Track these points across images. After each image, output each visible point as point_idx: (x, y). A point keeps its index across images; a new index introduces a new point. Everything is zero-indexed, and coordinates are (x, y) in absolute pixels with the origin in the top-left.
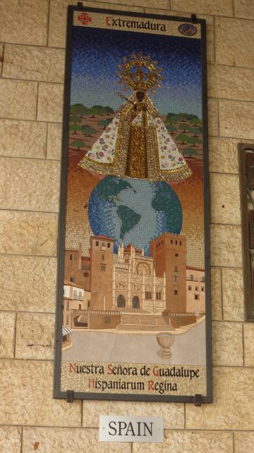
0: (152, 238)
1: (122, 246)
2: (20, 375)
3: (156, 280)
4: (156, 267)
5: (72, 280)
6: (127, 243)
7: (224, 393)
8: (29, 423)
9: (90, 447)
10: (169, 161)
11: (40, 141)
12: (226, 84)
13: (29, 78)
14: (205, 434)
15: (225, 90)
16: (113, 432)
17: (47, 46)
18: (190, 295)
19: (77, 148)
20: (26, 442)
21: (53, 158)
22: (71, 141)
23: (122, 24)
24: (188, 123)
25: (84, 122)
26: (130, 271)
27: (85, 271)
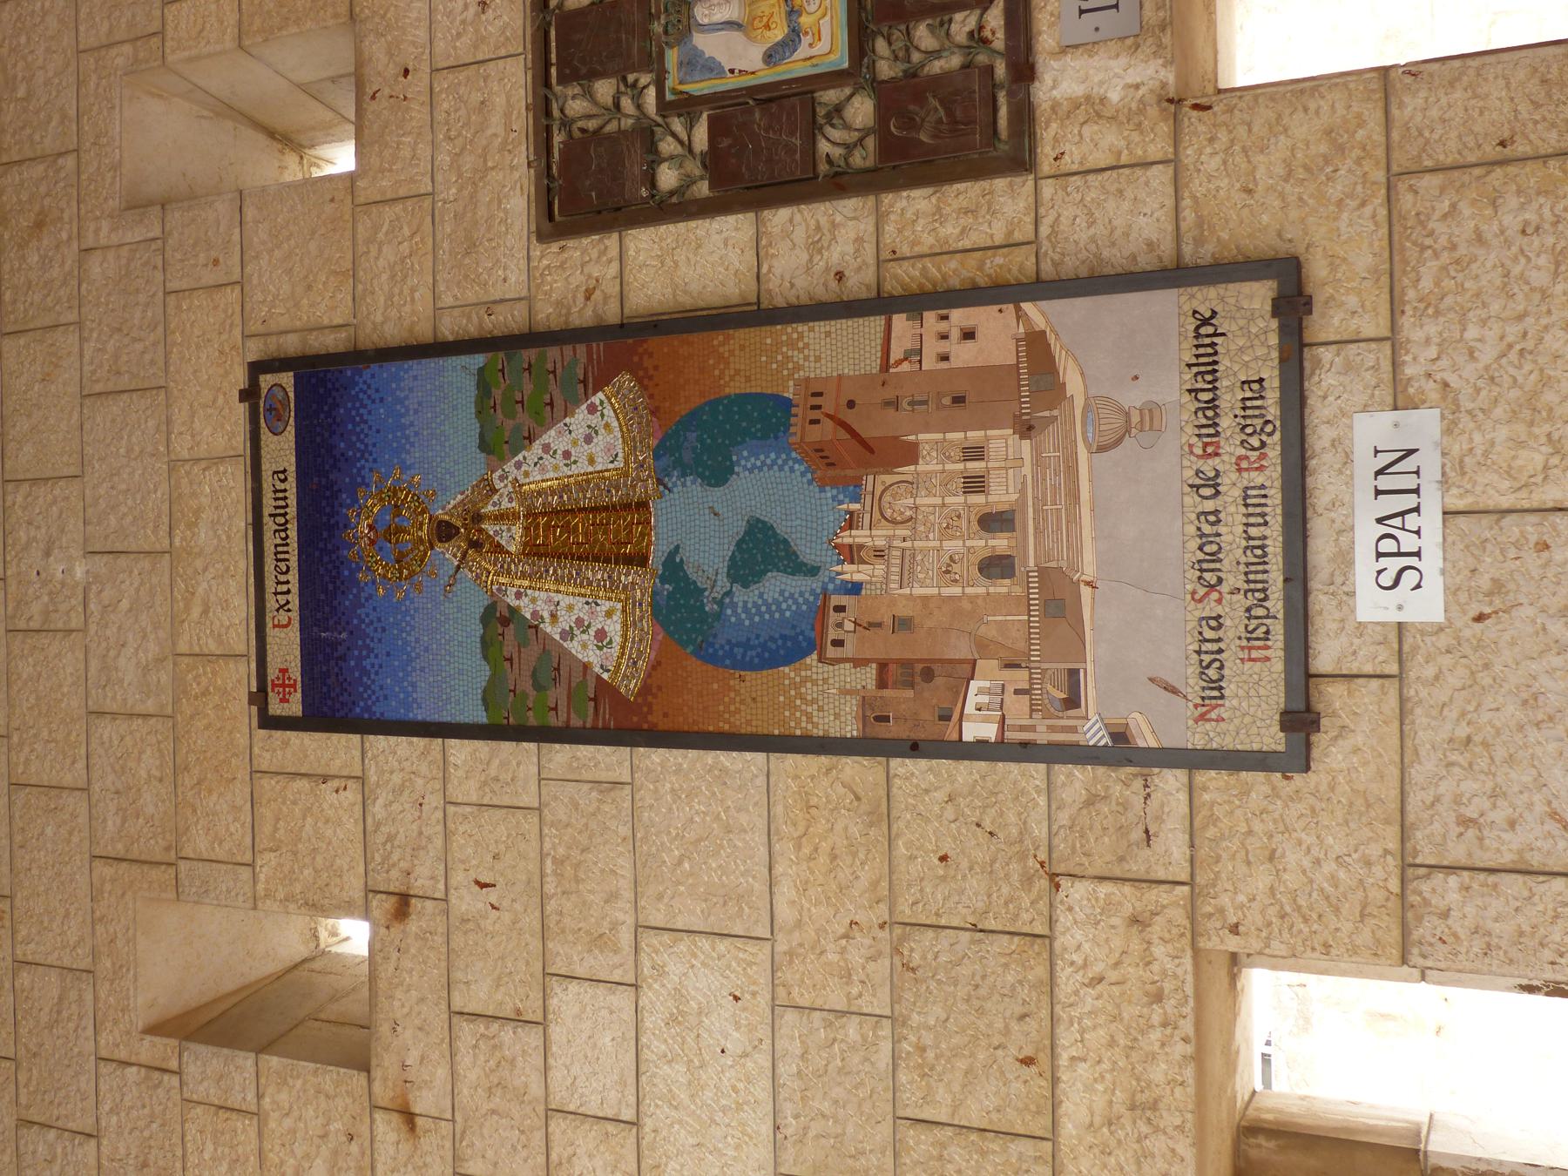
0: (810, 483)
1: (839, 568)
2: (1242, 869)
3: (928, 465)
4: (890, 465)
5: (946, 718)
6: (832, 555)
7: (1265, 218)
8: (1393, 845)
9: (1467, 650)
10: (600, 440)
11: (587, 798)
12: (396, 291)
13: (440, 828)
14: (1404, 272)
15: (413, 290)
16: (1410, 578)
17: (362, 779)
18: (964, 355)
19: (592, 703)
20: (1457, 853)
21: (627, 764)
22: (576, 722)
23: (284, 588)
24: (497, 393)
25: (526, 685)
26: (908, 544)
27: (918, 679)
